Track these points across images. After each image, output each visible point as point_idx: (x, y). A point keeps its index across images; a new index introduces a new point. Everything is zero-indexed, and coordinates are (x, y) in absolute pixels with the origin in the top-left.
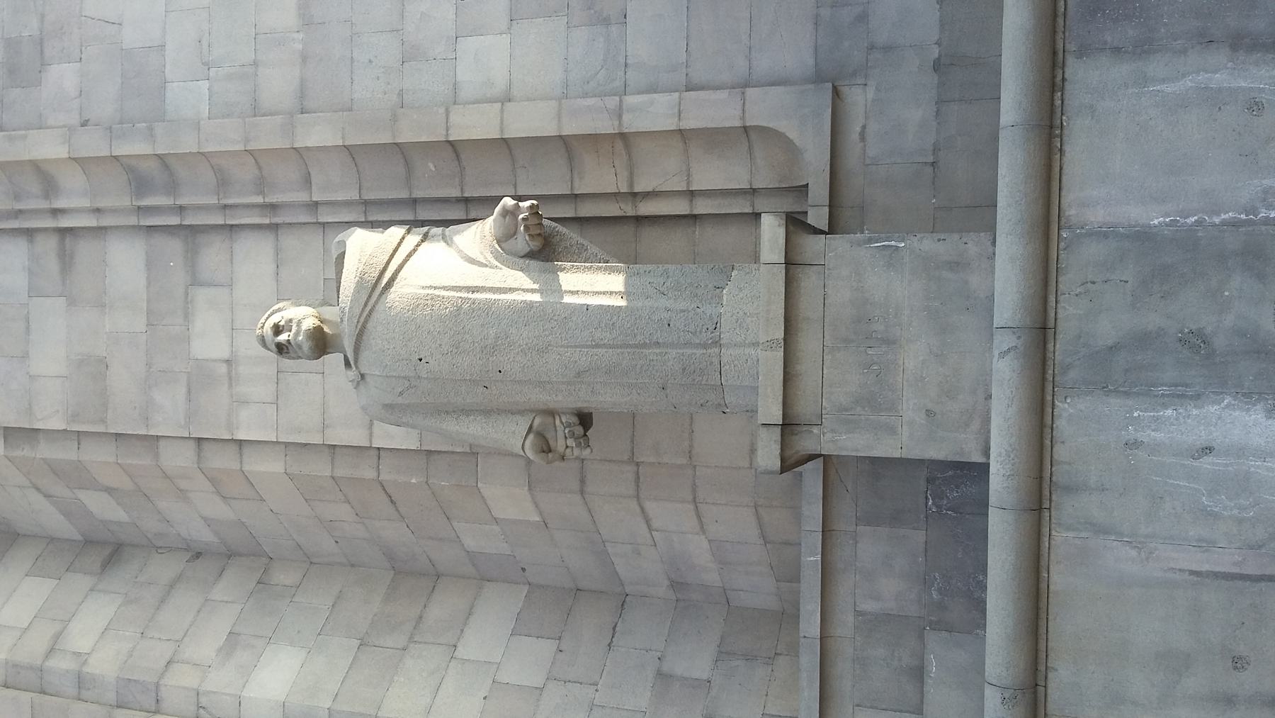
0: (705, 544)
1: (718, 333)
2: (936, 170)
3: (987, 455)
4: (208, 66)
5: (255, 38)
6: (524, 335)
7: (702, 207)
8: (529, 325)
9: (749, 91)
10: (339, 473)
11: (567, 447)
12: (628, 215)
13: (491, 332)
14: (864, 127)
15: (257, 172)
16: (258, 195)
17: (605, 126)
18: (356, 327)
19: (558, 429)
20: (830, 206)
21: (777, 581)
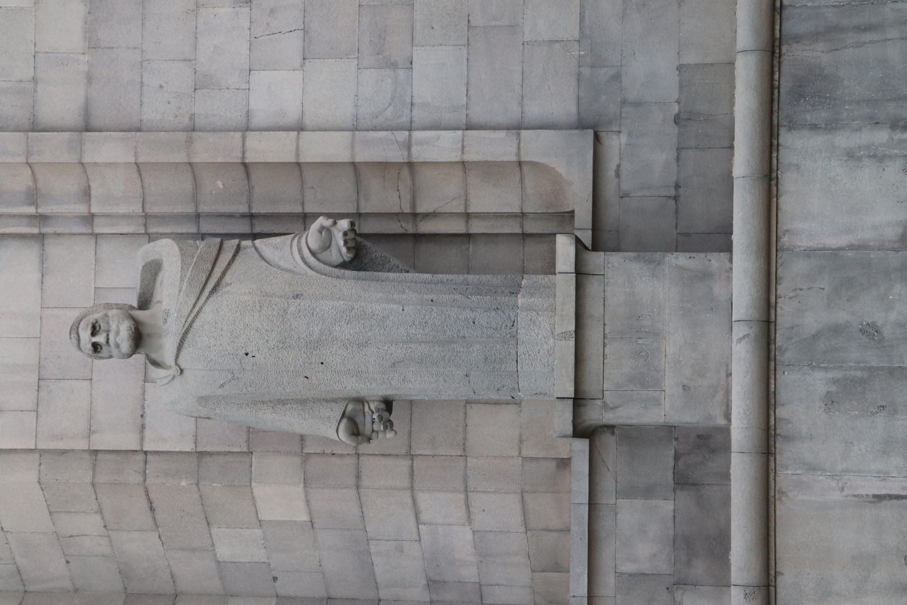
0: (469, 536)
1: (516, 329)
2: (677, 202)
3: (728, 416)
5: (34, 56)
7: (477, 227)
8: (351, 322)
9: (524, 133)
11: (373, 431)
12: (409, 232)
13: (316, 329)
14: (619, 166)
15: (31, 183)
17: (396, 155)
18: (184, 326)
19: (366, 415)
21: (532, 571)
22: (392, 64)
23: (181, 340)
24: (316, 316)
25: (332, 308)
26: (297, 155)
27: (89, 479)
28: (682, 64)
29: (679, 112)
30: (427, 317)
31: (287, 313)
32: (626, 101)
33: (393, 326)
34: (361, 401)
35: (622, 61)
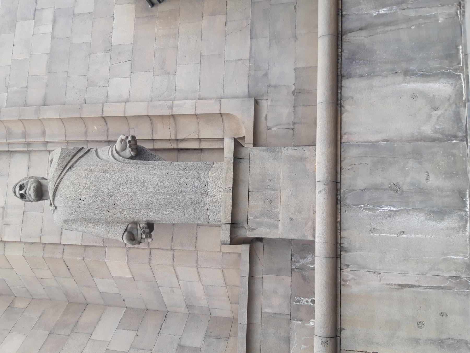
4: (7, 87)
6: (125, 188)
7: (204, 145)
9: (222, 100)
10: (46, 255)
11: (142, 238)
13: (112, 187)
14: (266, 115)
15: (23, 129)
16: (23, 138)
17: (167, 112)
19: (139, 230)
20: (253, 144)
22: (168, 73)
23: (54, 193)
24: (112, 181)
25: (120, 177)
26: (125, 113)
27: (41, 256)
28: (296, 68)
29: (295, 89)
30: (164, 181)
31: (99, 179)
32: (270, 85)
33: (148, 186)
34: (136, 223)
35: (268, 67)
